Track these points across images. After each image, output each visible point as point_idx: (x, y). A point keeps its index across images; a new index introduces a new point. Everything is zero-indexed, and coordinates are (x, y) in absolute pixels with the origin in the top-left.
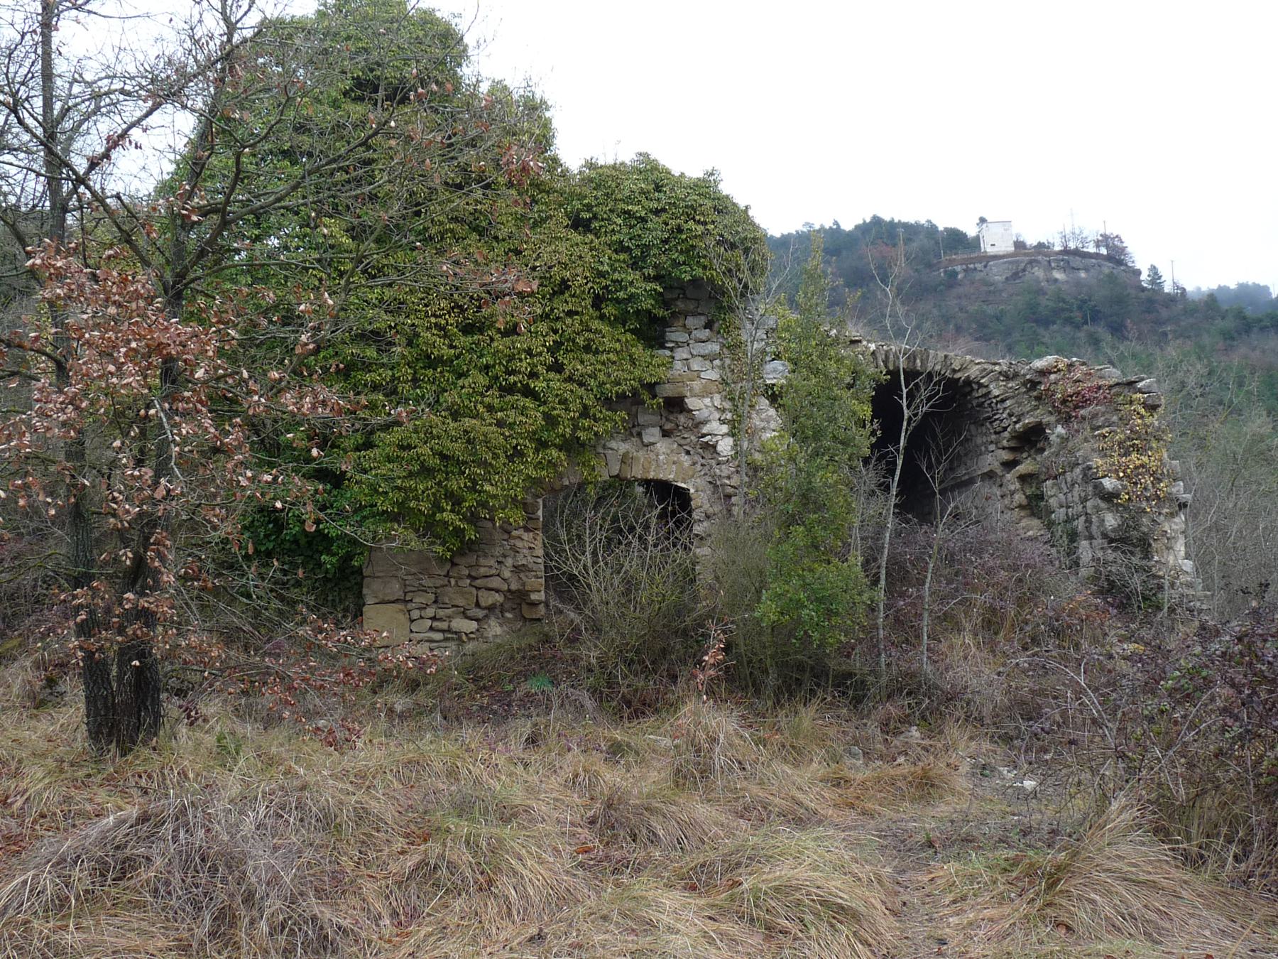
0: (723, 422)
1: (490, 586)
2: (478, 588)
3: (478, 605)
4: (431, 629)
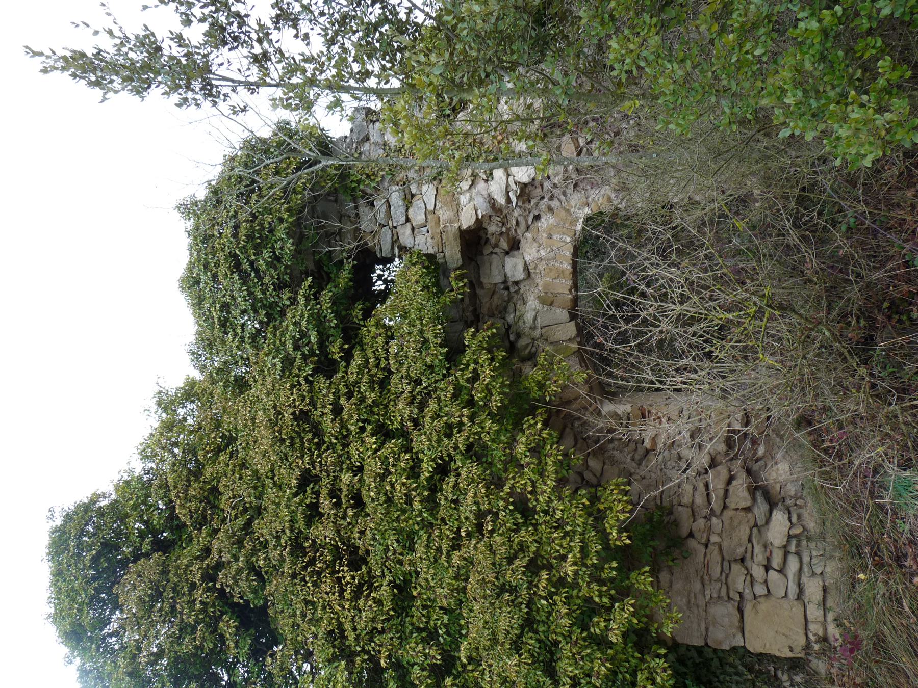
0: (490, 175)
1: (722, 492)
2: (725, 507)
3: (748, 509)
4: (781, 571)
